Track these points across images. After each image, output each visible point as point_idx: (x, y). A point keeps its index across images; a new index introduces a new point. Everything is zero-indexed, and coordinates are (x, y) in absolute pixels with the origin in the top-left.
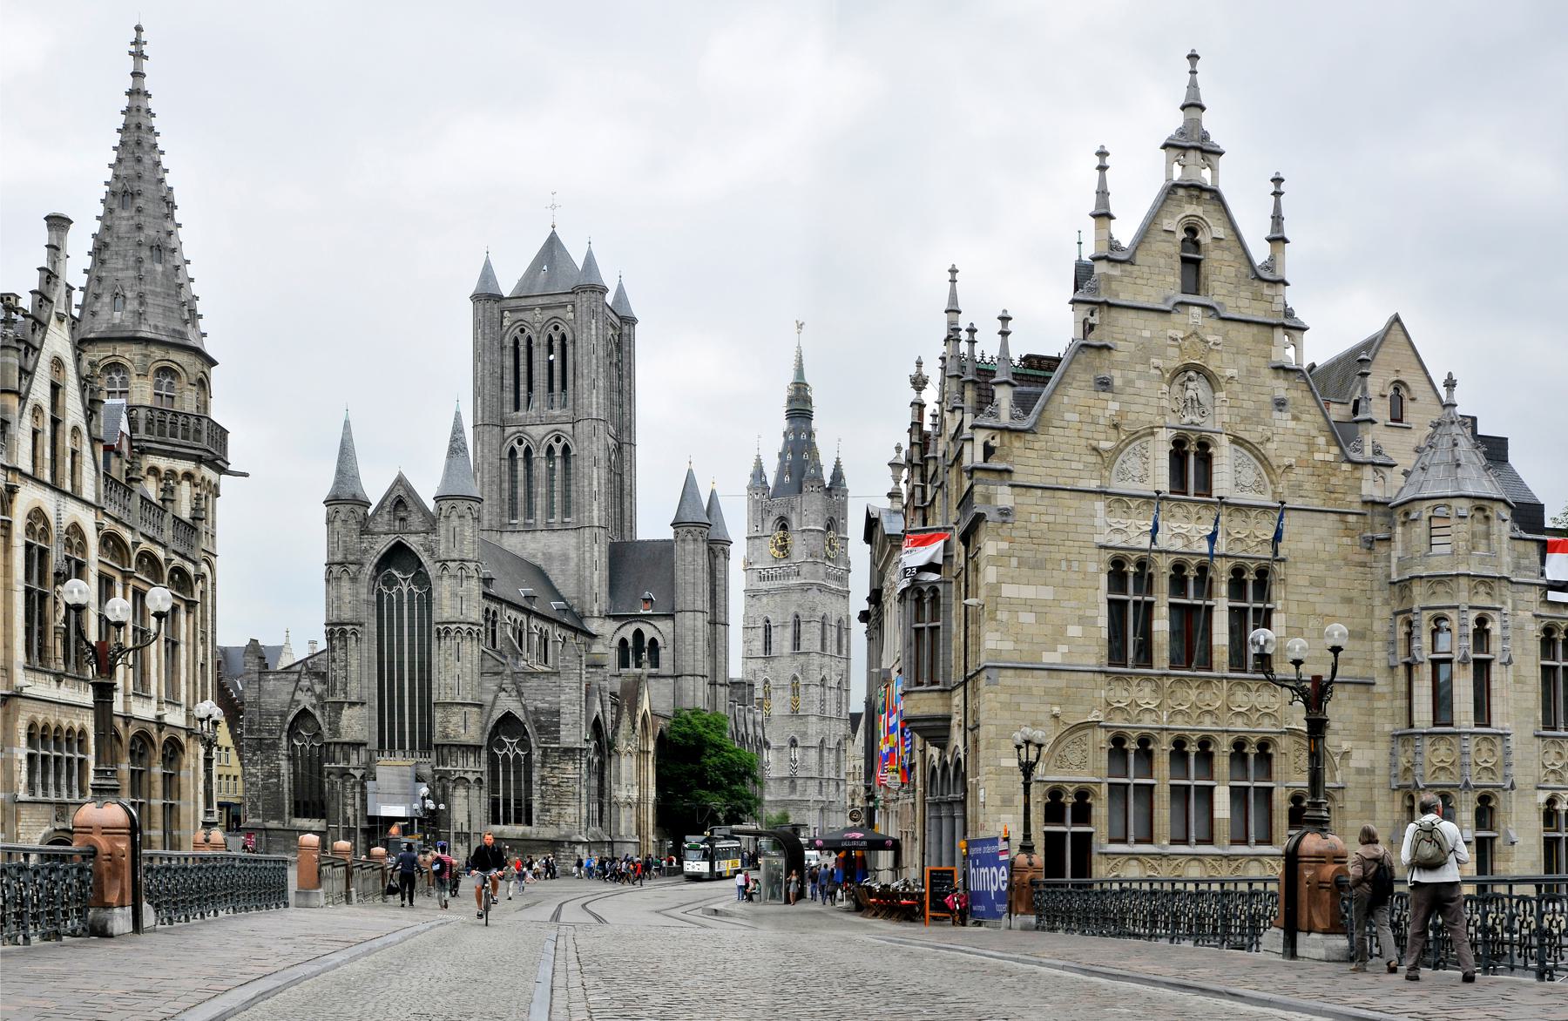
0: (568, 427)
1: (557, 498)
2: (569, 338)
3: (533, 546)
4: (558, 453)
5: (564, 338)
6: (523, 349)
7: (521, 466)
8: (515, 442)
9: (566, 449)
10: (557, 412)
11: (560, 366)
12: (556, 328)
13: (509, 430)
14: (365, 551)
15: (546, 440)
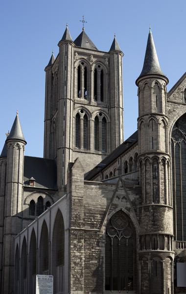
0: (106, 110)
1: (101, 140)
2: (106, 71)
3: (89, 160)
4: (100, 120)
5: (102, 71)
6: (83, 71)
7: (82, 123)
8: (80, 111)
9: (104, 119)
10: (100, 102)
11: (98, 82)
12: (99, 66)
13: (77, 105)
14: (170, 112)
15: (96, 112)
